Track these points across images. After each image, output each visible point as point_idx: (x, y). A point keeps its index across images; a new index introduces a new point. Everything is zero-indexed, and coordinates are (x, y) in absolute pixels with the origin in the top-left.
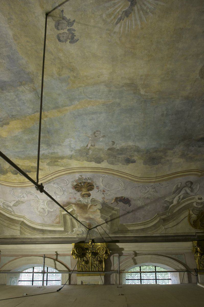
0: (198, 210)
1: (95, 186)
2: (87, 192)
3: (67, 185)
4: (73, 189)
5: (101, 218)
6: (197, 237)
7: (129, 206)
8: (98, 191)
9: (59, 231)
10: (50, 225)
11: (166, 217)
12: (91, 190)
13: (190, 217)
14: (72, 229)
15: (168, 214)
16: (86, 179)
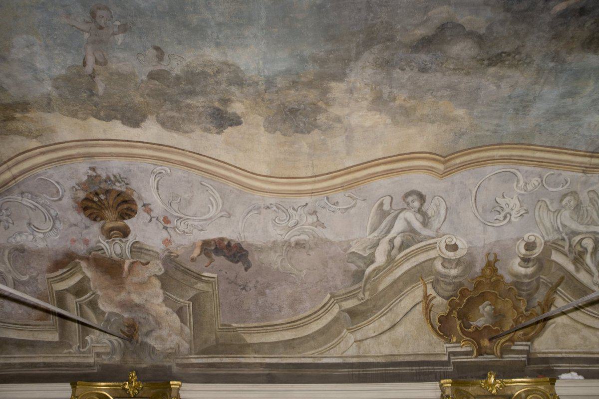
0: (450, 284)
2: (119, 224)
3: (60, 199)
4: (79, 213)
6: (451, 367)
7: (246, 270)
8: (150, 221)
9: (44, 341)
10: (20, 323)
12: (130, 217)
13: (428, 306)
14: (84, 337)
15: (363, 296)
16: (108, 178)
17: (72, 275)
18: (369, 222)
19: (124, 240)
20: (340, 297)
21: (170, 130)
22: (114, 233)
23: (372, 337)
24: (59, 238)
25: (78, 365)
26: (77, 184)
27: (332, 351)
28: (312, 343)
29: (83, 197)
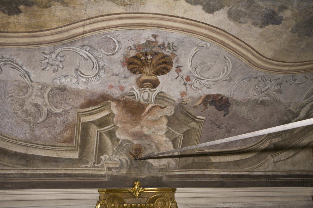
1: (175, 65)
2: (153, 78)
3: (113, 54)
4: (123, 66)
5: (165, 136)
7: (224, 116)
8: (177, 78)
9: (65, 159)
10: (47, 144)
11: (279, 141)
12: (163, 73)
14: (99, 156)
15: (284, 136)
16: (163, 45)
17: (101, 111)
18: (307, 93)
19: (152, 90)
20: (272, 136)
21: (232, 19)
22: (146, 84)
23: (283, 160)
24: (100, 83)
25: (93, 176)
26: (133, 45)
27: (260, 168)
28: (250, 163)
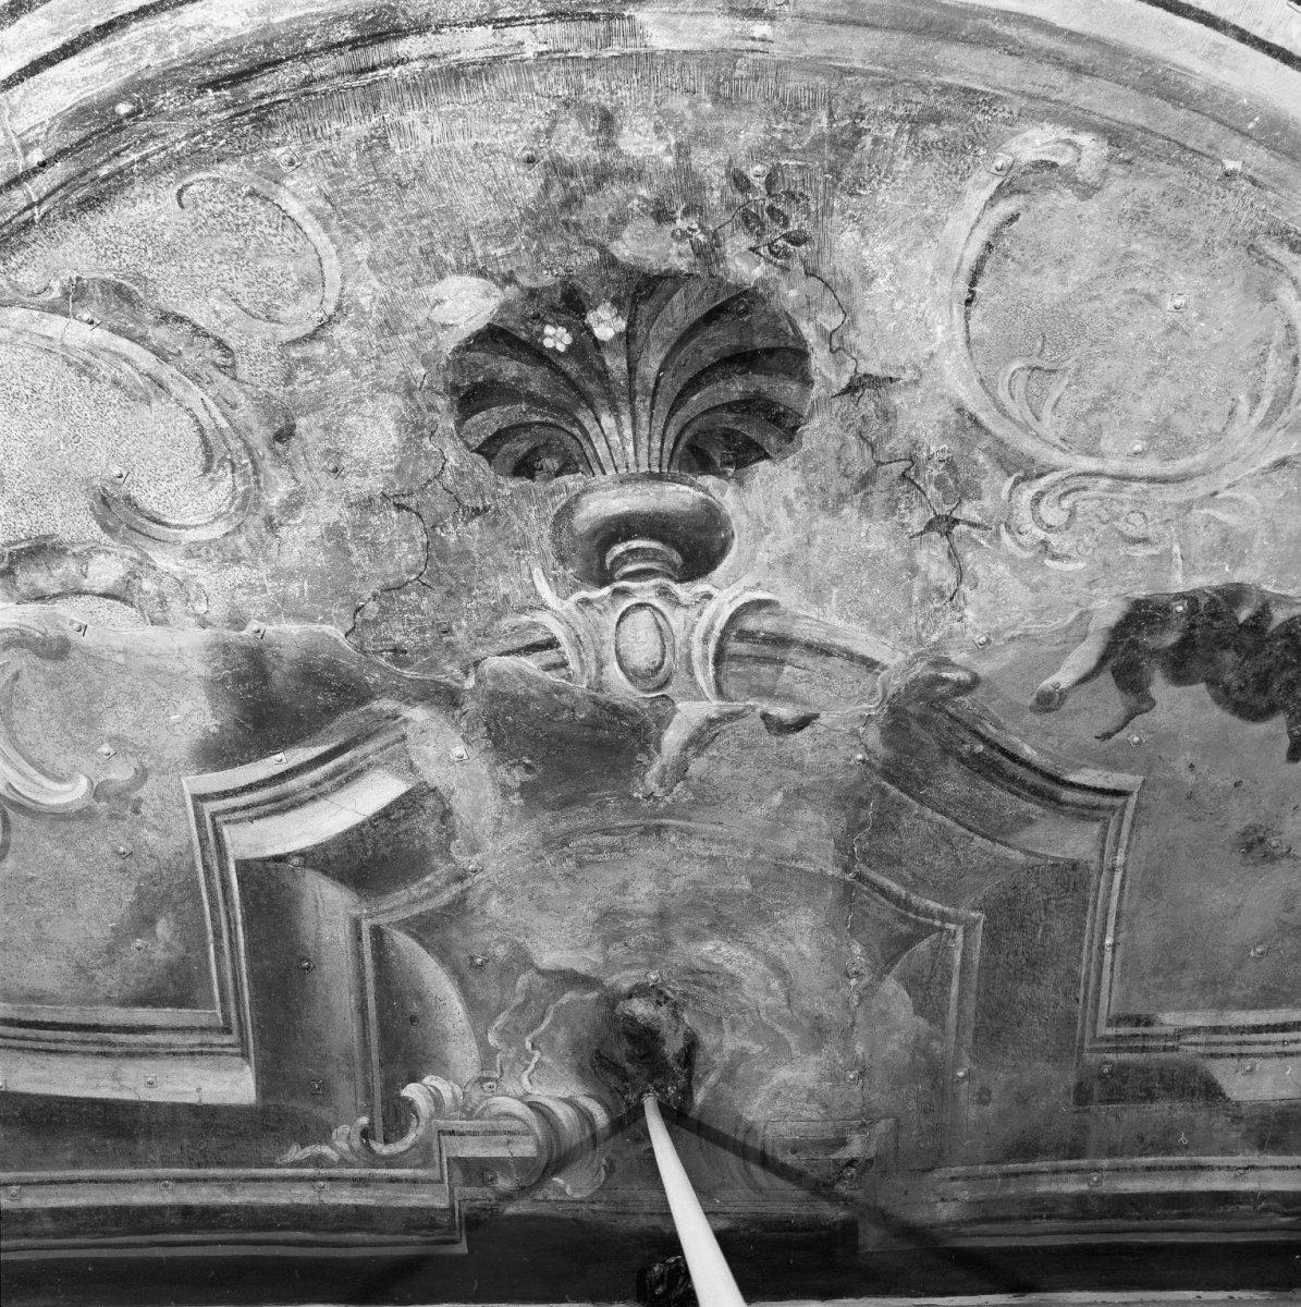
2: (678, 497)
12: (745, 454)
14: (392, 1086)
17: (348, 777)
19: (681, 591)
22: (631, 552)
25: (361, 1218)
29: (479, 324)
